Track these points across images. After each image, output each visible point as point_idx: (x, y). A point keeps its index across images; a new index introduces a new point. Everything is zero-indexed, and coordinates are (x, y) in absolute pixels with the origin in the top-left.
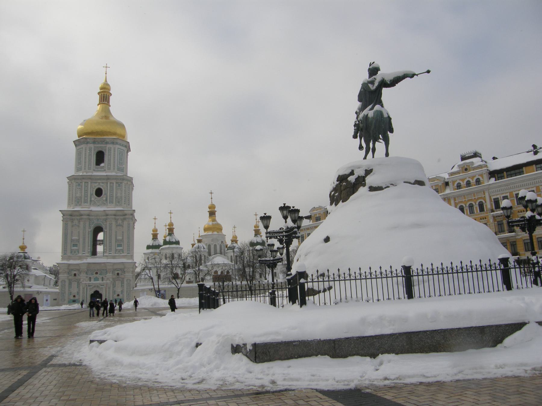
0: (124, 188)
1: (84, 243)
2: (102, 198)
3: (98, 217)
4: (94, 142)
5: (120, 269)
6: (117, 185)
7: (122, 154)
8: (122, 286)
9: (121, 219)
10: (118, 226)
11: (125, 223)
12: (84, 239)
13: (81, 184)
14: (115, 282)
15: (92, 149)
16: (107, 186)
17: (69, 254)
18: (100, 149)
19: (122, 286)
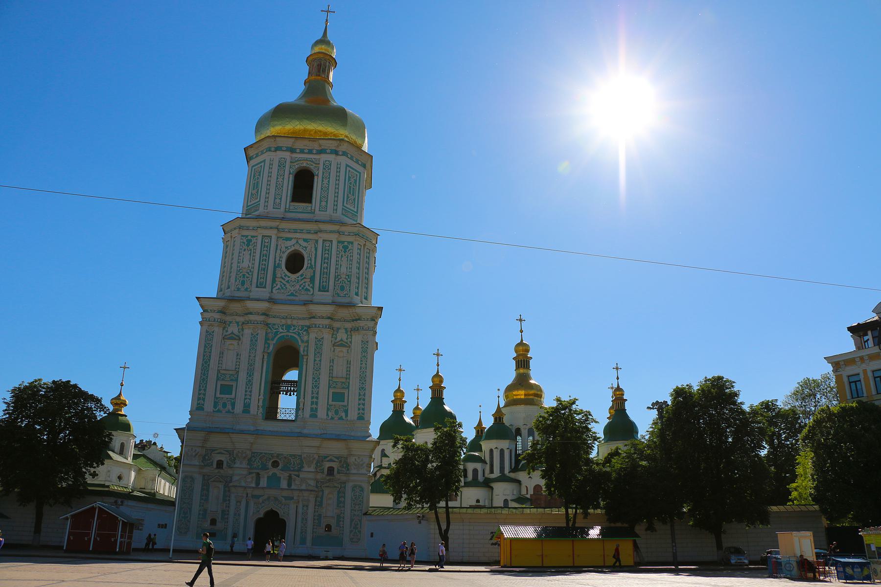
0: (356, 256)
1: (249, 383)
2: (302, 275)
3: (289, 322)
4: (292, 150)
5: (337, 458)
6: (341, 248)
7: (356, 181)
8: (340, 503)
9: (346, 329)
10: (338, 346)
11: (357, 338)
12: (250, 374)
13: (254, 240)
14: (323, 491)
15: (286, 162)
16: (316, 249)
17: (209, 406)
18: (305, 165)
19: (340, 503)
